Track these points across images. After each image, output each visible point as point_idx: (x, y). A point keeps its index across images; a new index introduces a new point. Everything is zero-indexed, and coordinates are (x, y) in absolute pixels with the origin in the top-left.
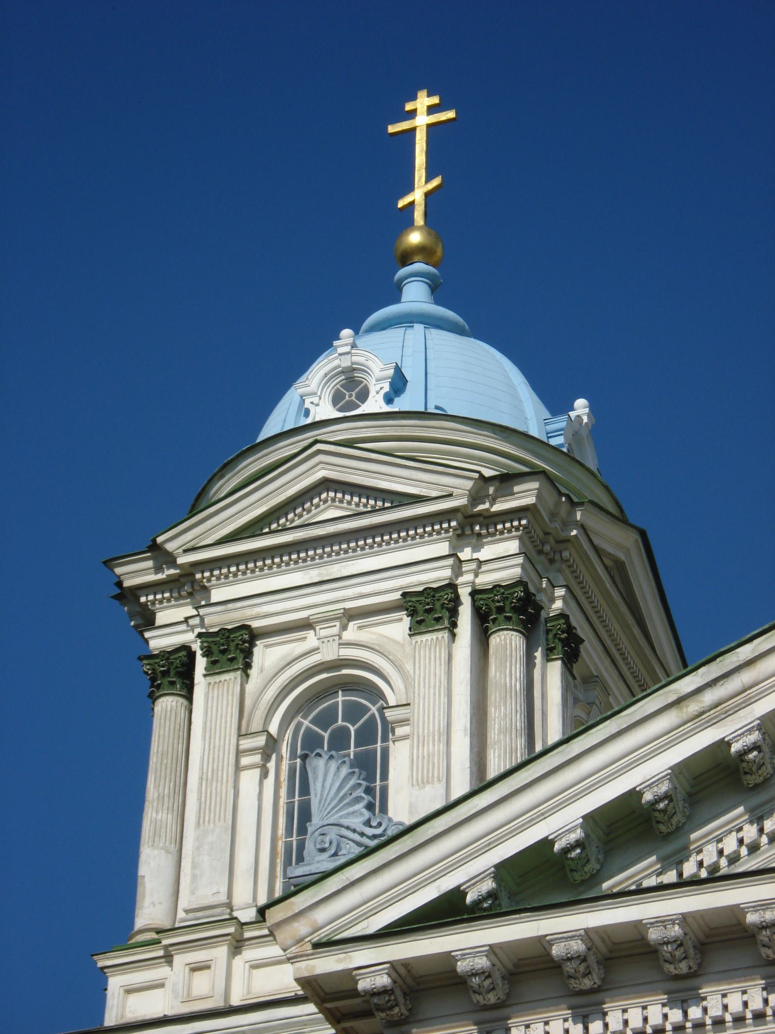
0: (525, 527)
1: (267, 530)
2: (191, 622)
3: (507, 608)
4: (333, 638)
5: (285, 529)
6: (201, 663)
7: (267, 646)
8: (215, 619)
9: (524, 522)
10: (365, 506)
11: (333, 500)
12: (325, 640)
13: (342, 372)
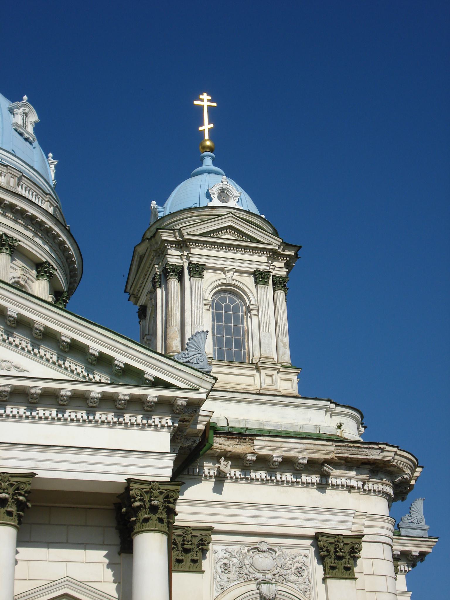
0: (287, 260)
1: (210, 236)
2: (183, 257)
6: (186, 272)
8: (194, 260)
9: (288, 259)
10: (241, 238)
11: (230, 232)
13: (222, 189)
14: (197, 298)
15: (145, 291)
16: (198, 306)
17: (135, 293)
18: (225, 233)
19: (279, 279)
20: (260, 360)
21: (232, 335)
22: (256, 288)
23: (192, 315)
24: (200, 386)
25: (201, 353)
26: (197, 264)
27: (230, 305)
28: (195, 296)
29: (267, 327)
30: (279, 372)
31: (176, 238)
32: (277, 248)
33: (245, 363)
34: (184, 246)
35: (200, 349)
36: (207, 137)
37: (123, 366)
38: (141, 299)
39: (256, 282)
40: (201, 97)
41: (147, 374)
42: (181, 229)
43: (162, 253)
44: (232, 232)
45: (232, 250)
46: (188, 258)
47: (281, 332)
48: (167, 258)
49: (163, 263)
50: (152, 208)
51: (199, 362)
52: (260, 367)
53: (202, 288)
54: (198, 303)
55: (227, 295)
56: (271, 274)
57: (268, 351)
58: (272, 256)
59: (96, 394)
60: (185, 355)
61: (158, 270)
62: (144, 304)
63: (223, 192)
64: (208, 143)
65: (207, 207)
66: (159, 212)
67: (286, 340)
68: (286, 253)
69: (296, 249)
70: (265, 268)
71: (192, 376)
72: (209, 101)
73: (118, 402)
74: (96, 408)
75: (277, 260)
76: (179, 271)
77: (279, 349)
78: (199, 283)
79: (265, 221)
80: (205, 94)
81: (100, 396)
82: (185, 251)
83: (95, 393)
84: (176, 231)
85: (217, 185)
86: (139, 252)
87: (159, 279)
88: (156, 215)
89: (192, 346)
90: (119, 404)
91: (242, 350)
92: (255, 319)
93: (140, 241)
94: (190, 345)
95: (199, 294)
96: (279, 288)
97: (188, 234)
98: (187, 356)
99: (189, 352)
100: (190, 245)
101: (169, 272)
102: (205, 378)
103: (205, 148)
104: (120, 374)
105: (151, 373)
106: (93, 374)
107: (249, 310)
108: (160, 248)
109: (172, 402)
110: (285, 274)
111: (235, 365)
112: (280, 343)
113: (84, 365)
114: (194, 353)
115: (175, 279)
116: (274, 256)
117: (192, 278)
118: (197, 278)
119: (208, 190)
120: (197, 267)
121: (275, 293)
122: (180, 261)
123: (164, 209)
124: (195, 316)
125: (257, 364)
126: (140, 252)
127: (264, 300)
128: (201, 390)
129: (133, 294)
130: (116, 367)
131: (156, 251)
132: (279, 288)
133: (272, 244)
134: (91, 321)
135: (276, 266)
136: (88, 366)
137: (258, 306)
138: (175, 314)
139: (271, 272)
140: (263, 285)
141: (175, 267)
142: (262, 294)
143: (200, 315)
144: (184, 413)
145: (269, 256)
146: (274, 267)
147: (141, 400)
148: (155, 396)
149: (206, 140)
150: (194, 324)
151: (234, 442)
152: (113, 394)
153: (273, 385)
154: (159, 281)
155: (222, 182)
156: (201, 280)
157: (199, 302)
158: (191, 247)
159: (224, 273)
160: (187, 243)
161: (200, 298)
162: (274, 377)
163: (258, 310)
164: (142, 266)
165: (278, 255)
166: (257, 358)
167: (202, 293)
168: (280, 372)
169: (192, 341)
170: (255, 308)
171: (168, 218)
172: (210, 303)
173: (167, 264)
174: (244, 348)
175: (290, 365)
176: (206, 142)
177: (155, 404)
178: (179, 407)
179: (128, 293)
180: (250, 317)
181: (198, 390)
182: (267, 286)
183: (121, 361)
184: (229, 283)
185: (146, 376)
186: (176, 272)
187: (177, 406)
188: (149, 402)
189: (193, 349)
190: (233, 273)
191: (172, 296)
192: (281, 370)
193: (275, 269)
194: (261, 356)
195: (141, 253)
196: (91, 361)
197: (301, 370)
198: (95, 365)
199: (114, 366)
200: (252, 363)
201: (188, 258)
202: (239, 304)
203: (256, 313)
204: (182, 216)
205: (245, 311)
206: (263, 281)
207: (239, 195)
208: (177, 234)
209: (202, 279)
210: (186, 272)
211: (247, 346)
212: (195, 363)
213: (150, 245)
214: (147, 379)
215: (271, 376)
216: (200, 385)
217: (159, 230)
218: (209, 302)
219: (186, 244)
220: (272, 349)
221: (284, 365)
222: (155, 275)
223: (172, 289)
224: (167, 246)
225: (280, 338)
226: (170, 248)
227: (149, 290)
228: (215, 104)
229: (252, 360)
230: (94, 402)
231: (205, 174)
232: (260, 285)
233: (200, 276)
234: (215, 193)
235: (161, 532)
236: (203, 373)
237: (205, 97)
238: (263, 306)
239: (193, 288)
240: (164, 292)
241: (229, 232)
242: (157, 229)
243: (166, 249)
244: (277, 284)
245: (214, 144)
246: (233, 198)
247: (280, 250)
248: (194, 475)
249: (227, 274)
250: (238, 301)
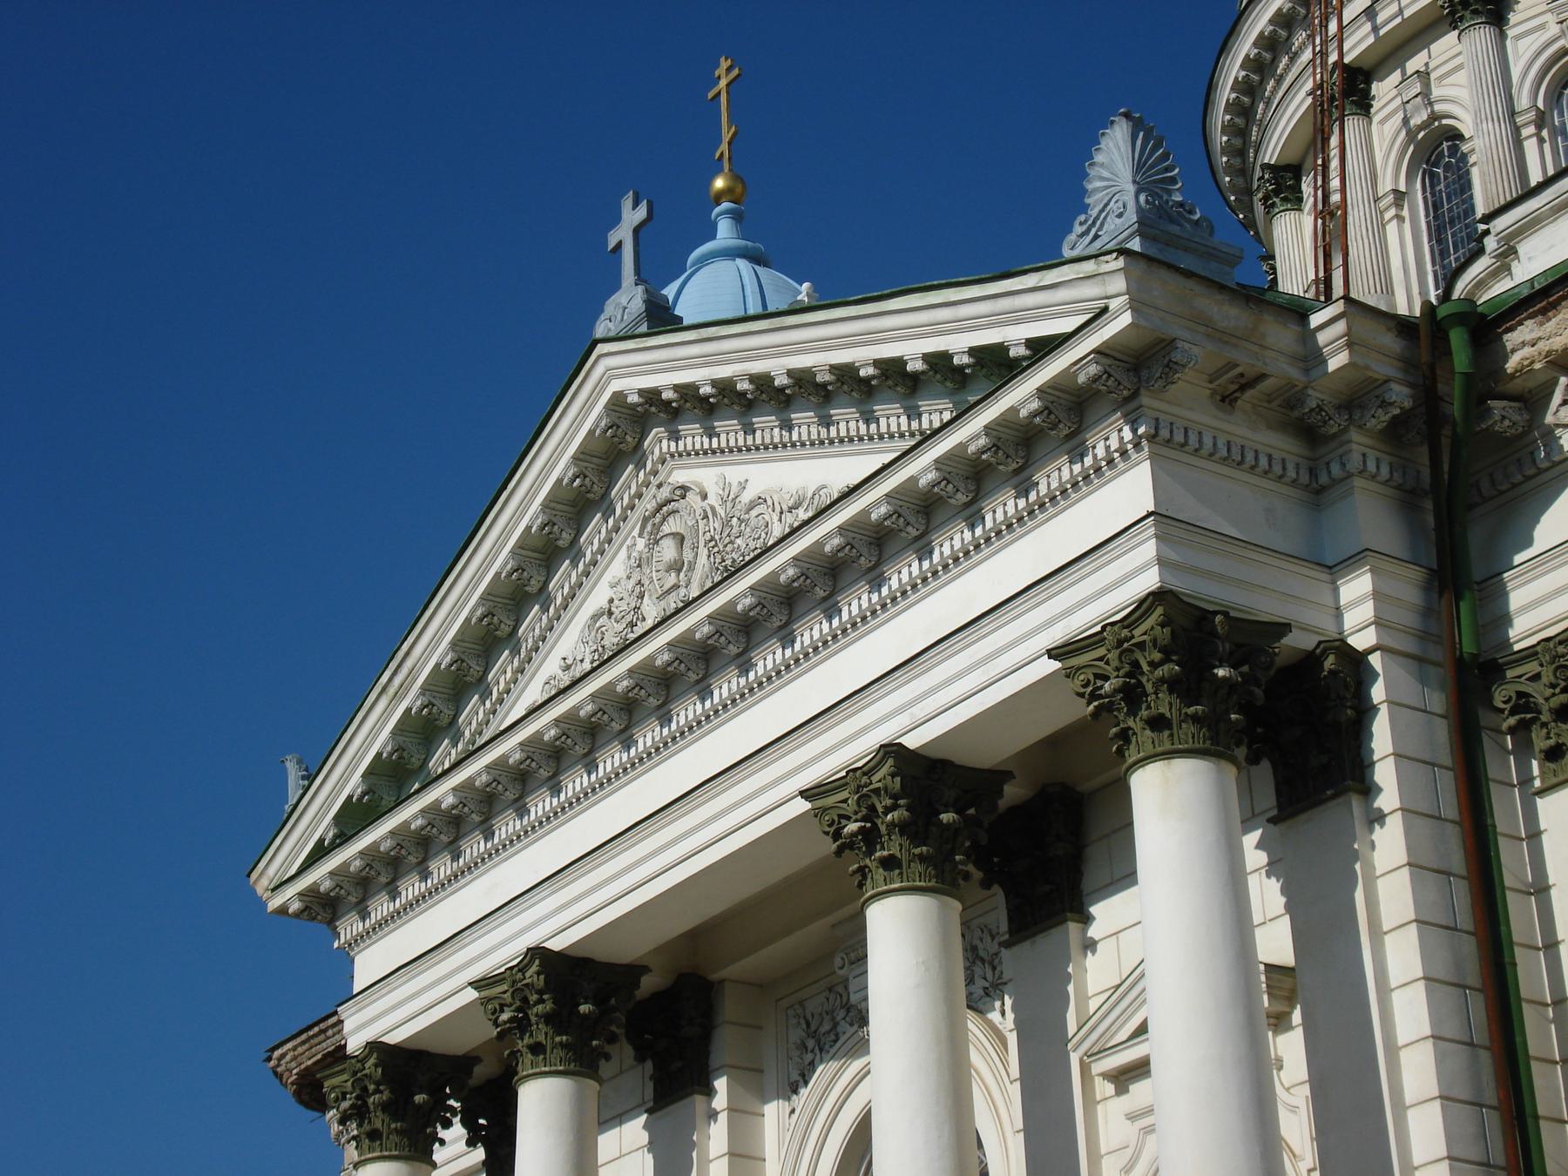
71: (1080, 282)
102: (1105, 268)
105: (1015, 335)
113: (947, 401)
128: (1114, 304)
148: (1032, 396)
151: (1564, 314)
183: (960, 350)
216: (1104, 295)
235: (1157, 758)
236: (1096, 256)
248: (1541, 471)
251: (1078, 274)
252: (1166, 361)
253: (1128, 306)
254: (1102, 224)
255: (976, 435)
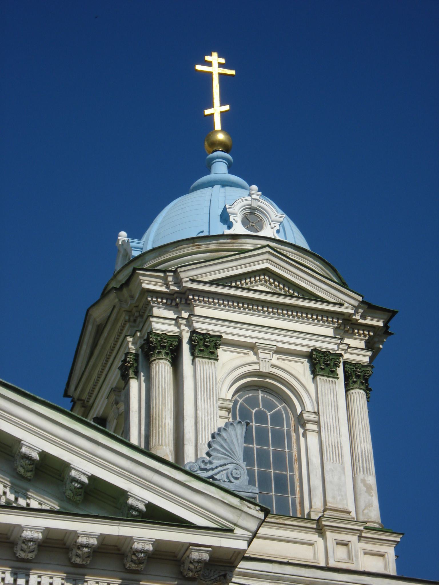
2: (181, 321)
3: (362, 377)
4: (268, 360)
5: (236, 287)
6: (186, 348)
7: (223, 350)
8: (201, 326)
9: (371, 334)
10: (285, 291)
11: (266, 281)
12: (264, 360)
13: (250, 208)
14: (207, 396)
15: (106, 390)
16: (209, 410)
17: (84, 397)
18: (256, 282)
19: (356, 368)
20: (325, 513)
21: (270, 467)
22: (313, 383)
23: (198, 426)
24: (235, 525)
25: (234, 461)
26: (207, 335)
27: (265, 412)
28: (202, 392)
29: (335, 453)
30: (360, 537)
31: (168, 288)
32: (352, 311)
33: (295, 517)
34: (183, 301)
35: (234, 454)
36: (218, 125)
37: (86, 480)
38: (95, 405)
39: (314, 372)
40: (207, 58)
41: (134, 497)
42: (179, 270)
43: (141, 316)
44: (269, 280)
45: (269, 313)
46: (189, 322)
47: (361, 465)
48: (151, 322)
49: (143, 333)
50: (120, 243)
51: (232, 479)
52: (326, 527)
53: (216, 379)
54: (207, 405)
55: (260, 394)
56: (341, 358)
57: (339, 498)
58: (342, 328)
59: (33, 532)
60: (206, 464)
61: (132, 347)
62: (103, 413)
63: (252, 213)
64: (221, 137)
65: (223, 236)
66: (133, 249)
67: (372, 480)
68: (369, 321)
69: (387, 316)
70: (331, 346)
71: (220, 504)
72: (221, 65)
73: (75, 551)
74: (32, 562)
75: (352, 335)
76: (172, 346)
77: (358, 496)
78: (209, 369)
79: (328, 266)
80: (215, 55)
81: (40, 536)
82: (183, 312)
83: (31, 531)
84: (168, 274)
85: (240, 200)
86: (95, 319)
87: (134, 362)
88: (127, 254)
89: (218, 448)
90: (77, 556)
91: (290, 496)
92: (312, 439)
93: (98, 297)
94: (215, 446)
95: (210, 389)
96: (356, 386)
97: (191, 280)
98: (208, 466)
99: (212, 459)
100: (193, 300)
101: (155, 348)
102: (246, 509)
103: (215, 145)
104: (78, 498)
106: (26, 497)
107: (301, 421)
108: (137, 307)
109: (179, 556)
110: (367, 360)
111: (277, 521)
112: (360, 486)
113: (9, 479)
114: (222, 462)
115: (165, 361)
116: (346, 326)
117: (197, 359)
118: (207, 360)
119: (225, 209)
120: (207, 340)
121: (349, 394)
122: (175, 329)
123: (143, 244)
124: (202, 428)
125: (318, 521)
126: (98, 320)
127: (329, 404)
128: (238, 531)
129: (79, 399)
130: (73, 483)
131: (129, 312)
132: (355, 385)
133: (343, 305)
134: (28, 393)
135: (349, 345)
136: (18, 482)
137: (319, 416)
138: (165, 423)
139: (341, 355)
140: (327, 376)
141: (166, 339)
142: (325, 394)
143: (212, 425)
144: (202, 578)
145: (337, 328)
146: (345, 347)
147: (119, 550)
148: (148, 541)
149: (217, 132)
150: (201, 442)
152: (65, 536)
153: (351, 561)
154: (135, 365)
155: (250, 195)
156: (214, 362)
157: (210, 403)
158: (194, 303)
159: (256, 354)
160: (188, 297)
161: (212, 395)
162: (352, 546)
163: (318, 423)
164: (101, 341)
165: (354, 326)
166: (318, 510)
167: (216, 387)
168: (362, 539)
169: (218, 439)
170: (314, 417)
171: (152, 255)
172: (230, 405)
173: (151, 333)
174: (293, 493)
175: (380, 527)
176: (217, 134)
177: (146, 557)
178: (194, 564)
179: (70, 399)
180: (304, 435)
181: (232, 531)
182: (334, 380)
183: (83, 471)
184: (264, 371)
185: (131, 501)
186: (167, 348)
187: (191, 563)
188: (136, 552)
189: (221, 454)
190: (271, 353)
191: (159, 390)
192: (364, 535)
193: (347, 350)
194: (327, 507)
195: (99, 321)
196: (22, 470)
197: (401, 536)
198: (30, 480)
199: (68, 482)
200: (309, 519)
201: (189, 322)
202: (281, 411)
203: (314, 427)
204: (177, 251)
205: (293, 424)
206: (328, 369)
207: (281, 219)
208: (170, 279)
209: (215, 362)
210: (186, 348)
211: (297, 489)
212: (224, 481)
213: (120, 300)
214: (132, 507)
215: (346, 544)
216: (235, 522)
217: (137, 271)
218: (228, 403)
219: (187, 299)
220: (346, 495)
221: (370, 526)
222: (127, 354)
223: (159, 378)
224: (151, 301)
225: (360, 476)
226: (156, 305)
227: (114, 386)
228: (233, 72)
229: (309, 514)
230: (28, 550)
231: (217, 187)
232: (322, 378)
233: (213, 356)
234: (237, 215)
237: (214, 58)
238: (328, 416)
239: (199, 377)
240: (143, 385)
241: (263, 282)
242: (135, 270)
243: (149, 308)
244: (352, 378)
245: (230, 139)
246: (270, 224)
247: (357, 317)
249: (261, 355)
250: (280, 407)
251: (222, 498)
252: (222, 573)
253: (248, 539)
254: (219, 473)
255: (90, 535)
